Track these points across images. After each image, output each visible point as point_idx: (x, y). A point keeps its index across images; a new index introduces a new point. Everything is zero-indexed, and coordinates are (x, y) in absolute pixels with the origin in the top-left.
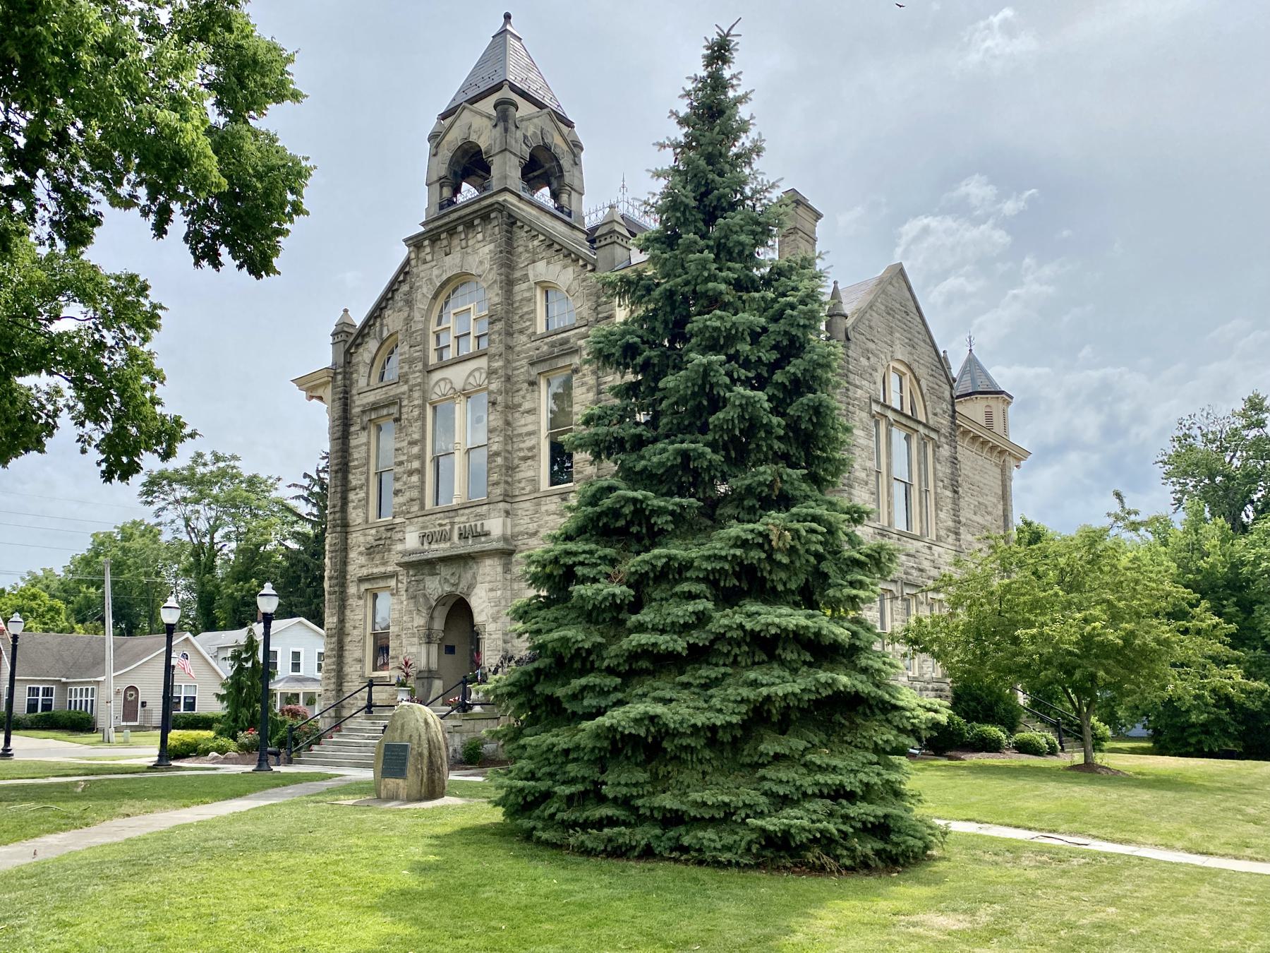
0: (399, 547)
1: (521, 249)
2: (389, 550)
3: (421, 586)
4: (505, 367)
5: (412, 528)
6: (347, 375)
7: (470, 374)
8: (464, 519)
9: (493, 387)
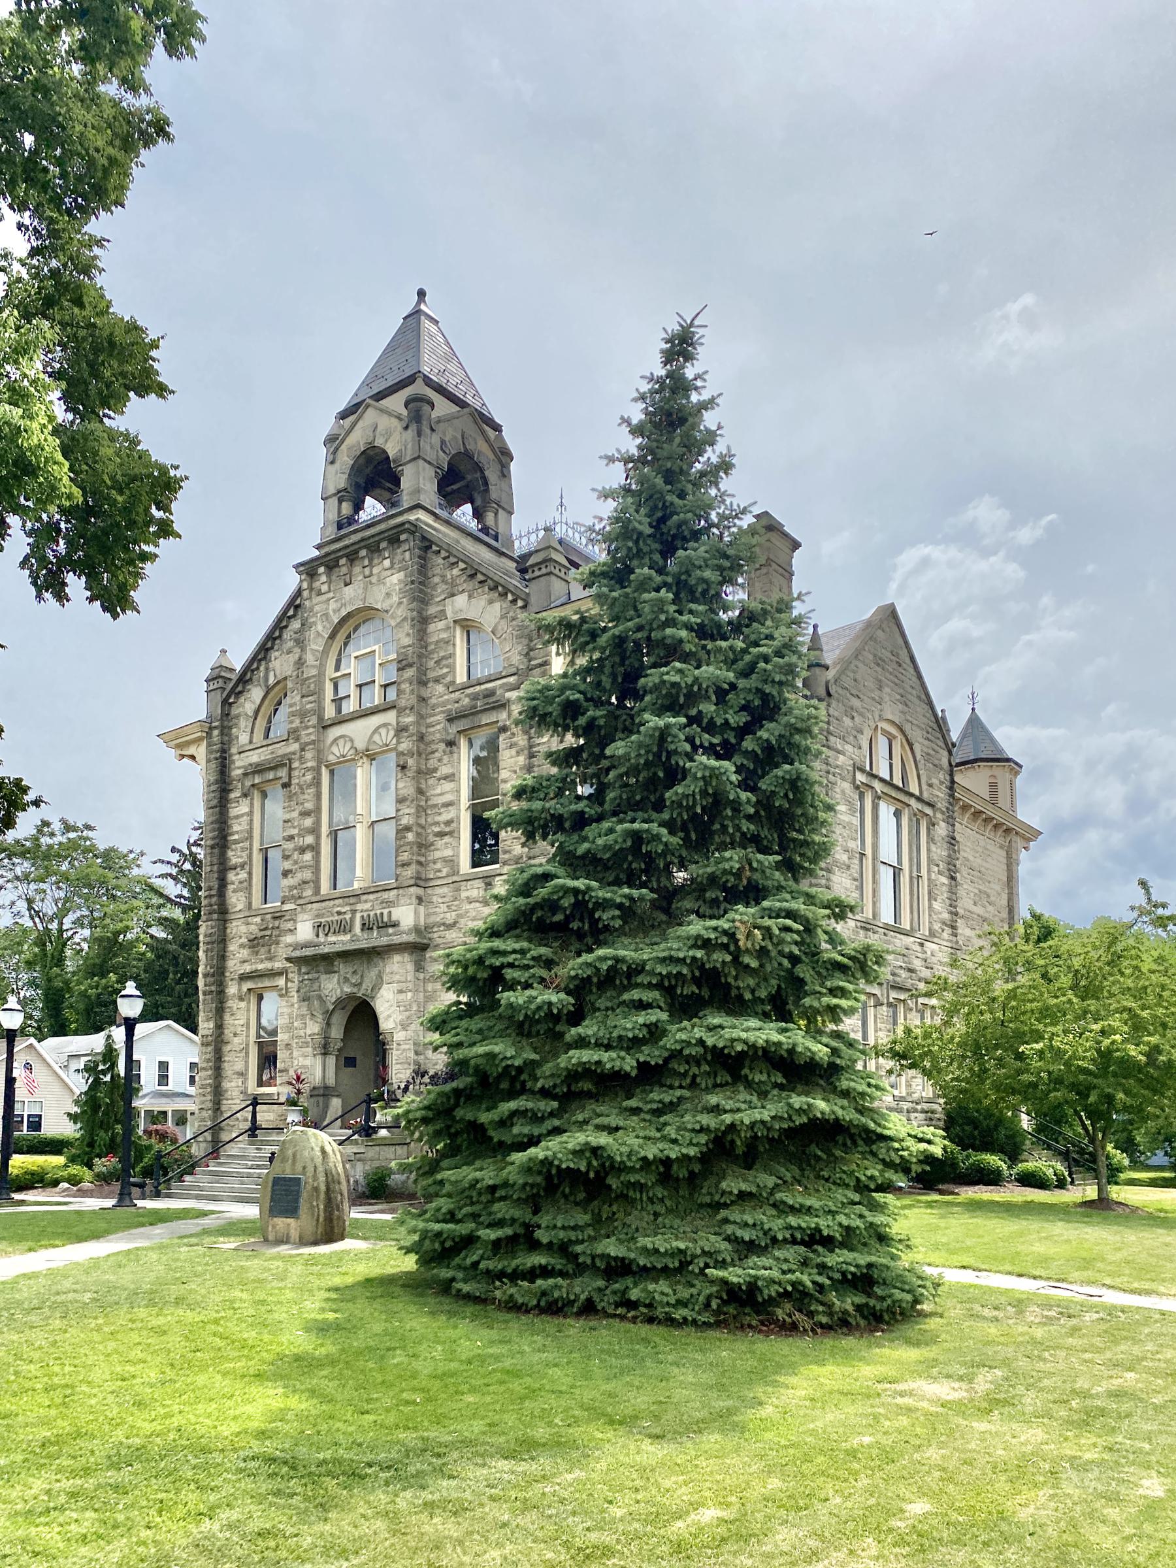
0: (289, 939)
1: (437, 579)
3: (315, 987)
4: (418, 723)
5: (306, 917)
6: (225, 730)
7: (376, 730)
9: (404, 746)
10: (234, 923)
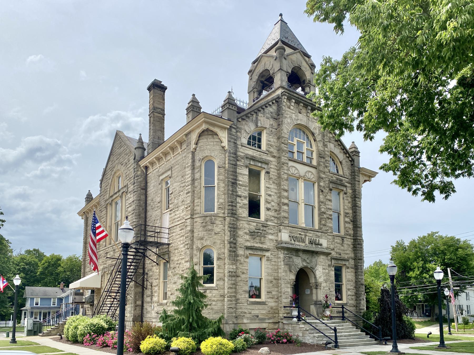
0: (270, 237)
2: (265, 237)
3: (291, 260)
8: (311, 235)
10: (241, 222)
